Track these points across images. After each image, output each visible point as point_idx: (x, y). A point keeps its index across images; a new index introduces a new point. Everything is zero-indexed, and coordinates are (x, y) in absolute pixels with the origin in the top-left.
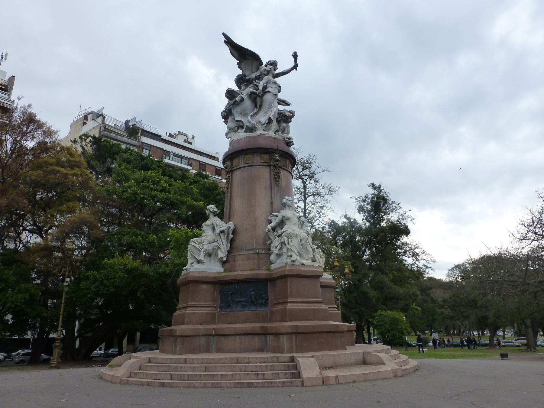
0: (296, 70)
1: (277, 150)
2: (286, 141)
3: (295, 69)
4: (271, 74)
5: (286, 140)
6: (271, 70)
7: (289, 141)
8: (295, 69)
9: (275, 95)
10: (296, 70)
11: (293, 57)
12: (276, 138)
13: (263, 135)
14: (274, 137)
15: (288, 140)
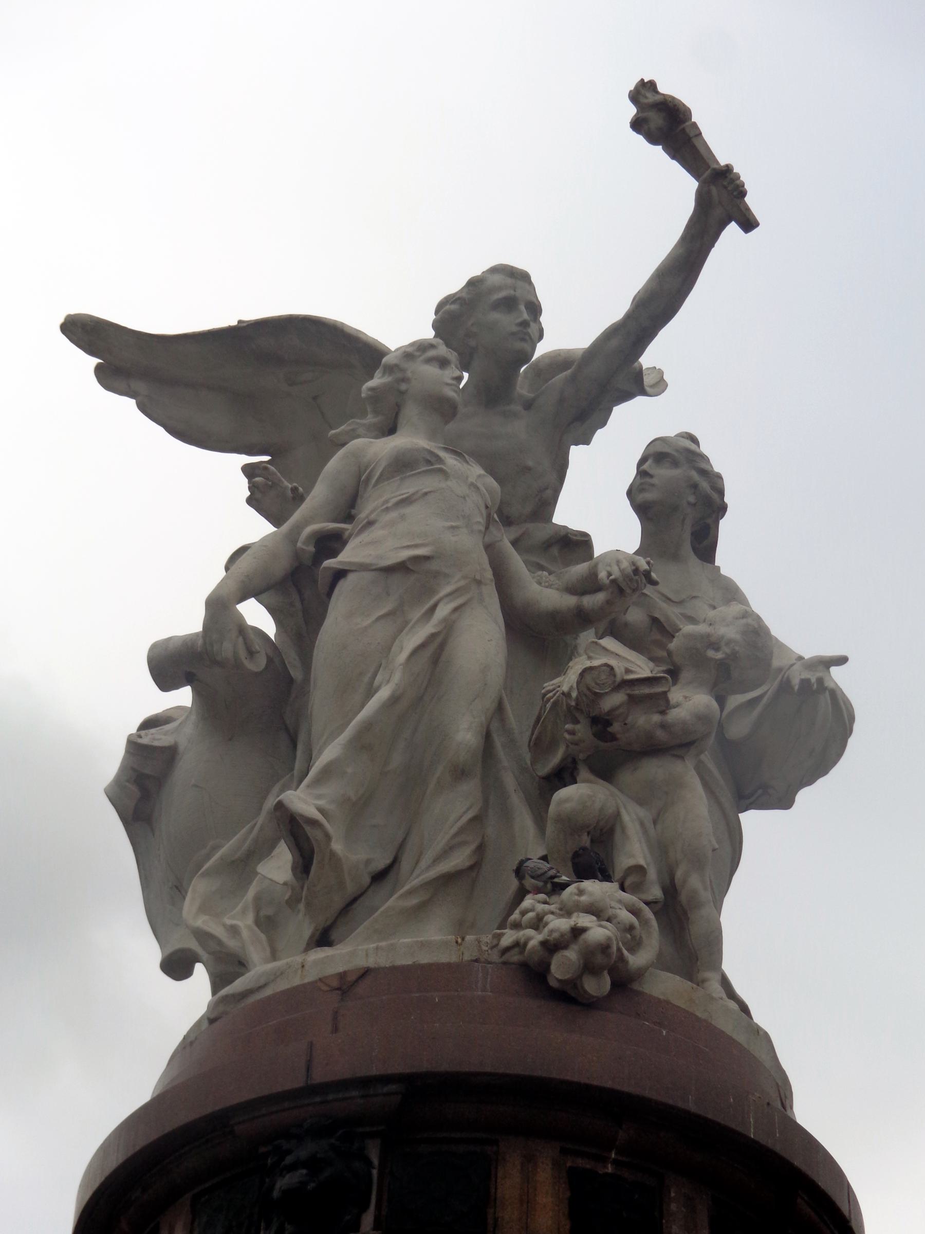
0: (748, 224)
1: (311, 1090)
2: (515, 957)
3: (732, 230)
4: (411, 412)
5: (516, 944)
6: (404, 380)
7: (535, 938)
8: (732, 230)
9: (402, 568)
10: (748, 224)
11: (653, 139)
12: (366, 973)
13: (251, 999)
14: (342, 976)
15: (530, 932)
